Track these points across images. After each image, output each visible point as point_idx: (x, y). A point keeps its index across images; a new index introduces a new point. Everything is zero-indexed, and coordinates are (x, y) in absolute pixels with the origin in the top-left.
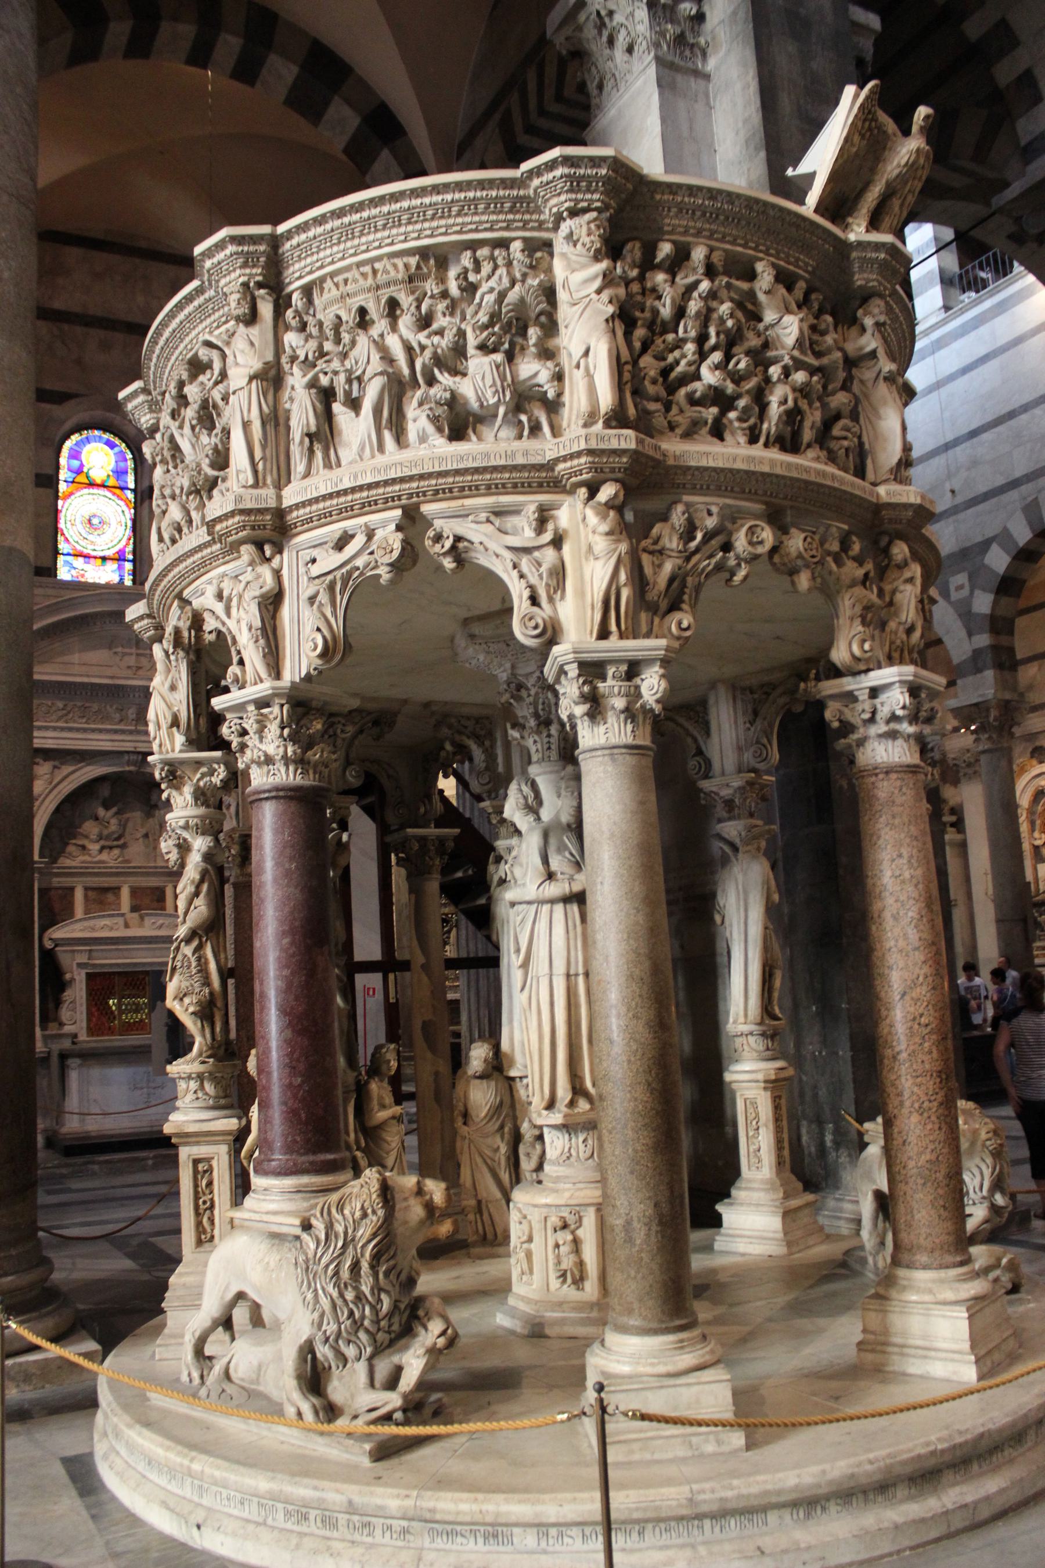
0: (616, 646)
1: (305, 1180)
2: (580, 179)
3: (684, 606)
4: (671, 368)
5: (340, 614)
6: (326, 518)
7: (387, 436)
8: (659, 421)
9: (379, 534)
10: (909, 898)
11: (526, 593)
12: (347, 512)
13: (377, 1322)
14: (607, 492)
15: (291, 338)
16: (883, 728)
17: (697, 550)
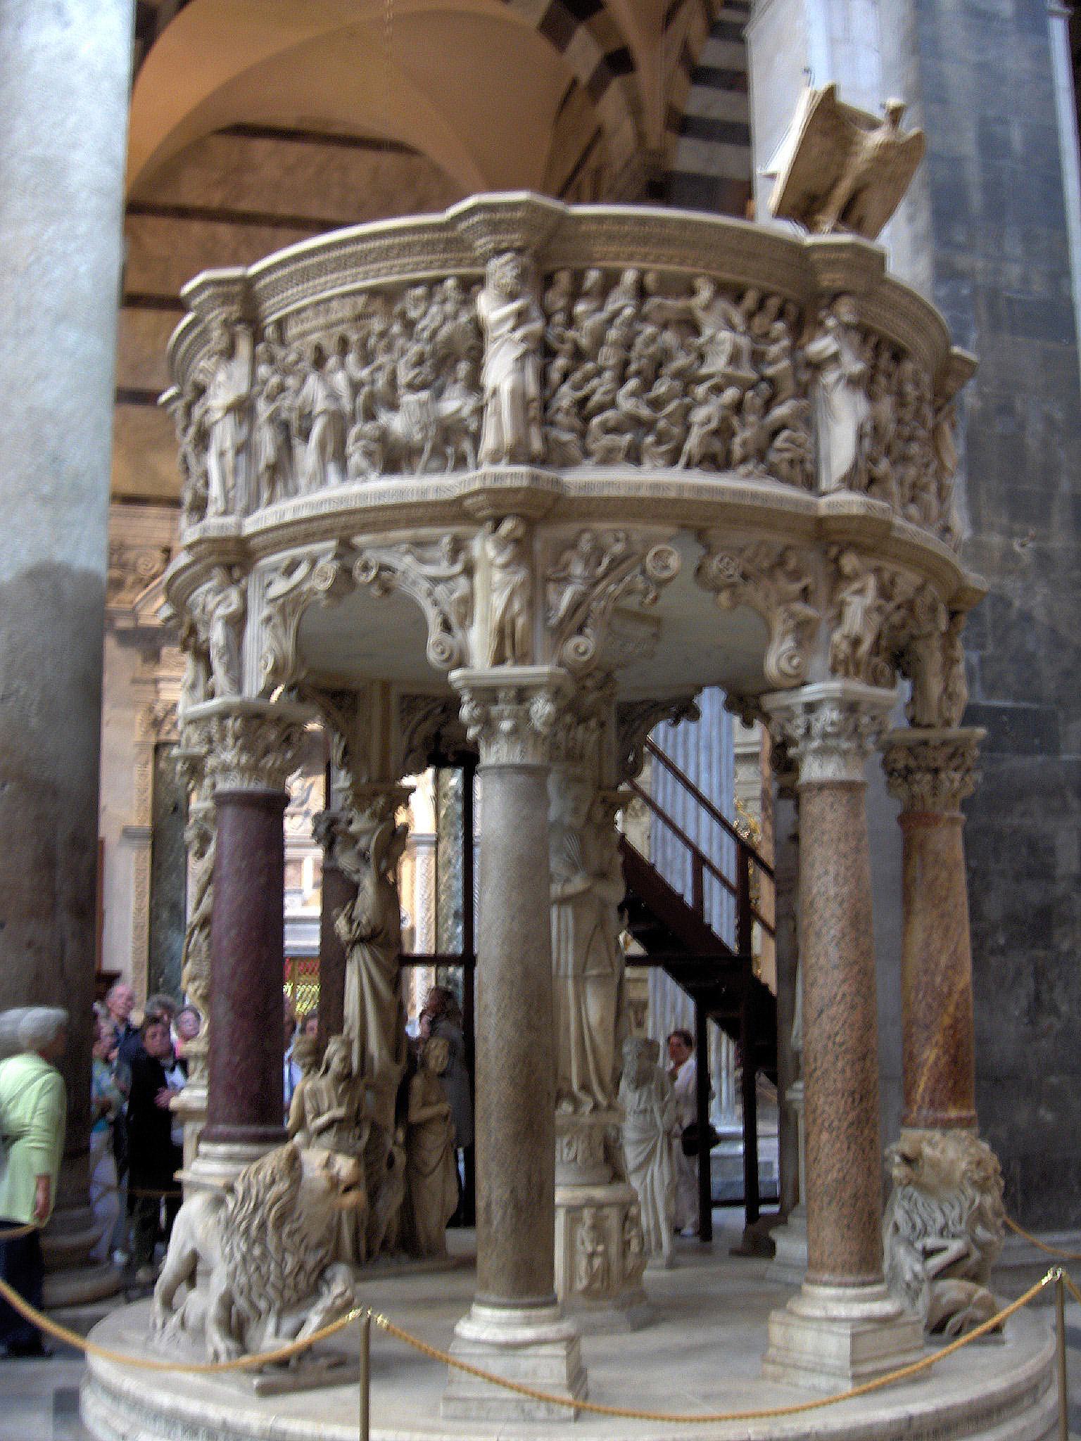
0: (509, 671)
1: (236, 1148)
2: (501, 222)
3: (588, 631)
4: (586, 399)
5: (292, 632)
6: (277, 547)
7: (332, 469)
8: (575, 451)
9: (321, 563)
10: (832, 916)
11: (439, 620)
12: (293, 542)
13: (282, 1277)
14: (507, 526)
15: (263, 370)
16: (816, 744)
17: (606, 575)
